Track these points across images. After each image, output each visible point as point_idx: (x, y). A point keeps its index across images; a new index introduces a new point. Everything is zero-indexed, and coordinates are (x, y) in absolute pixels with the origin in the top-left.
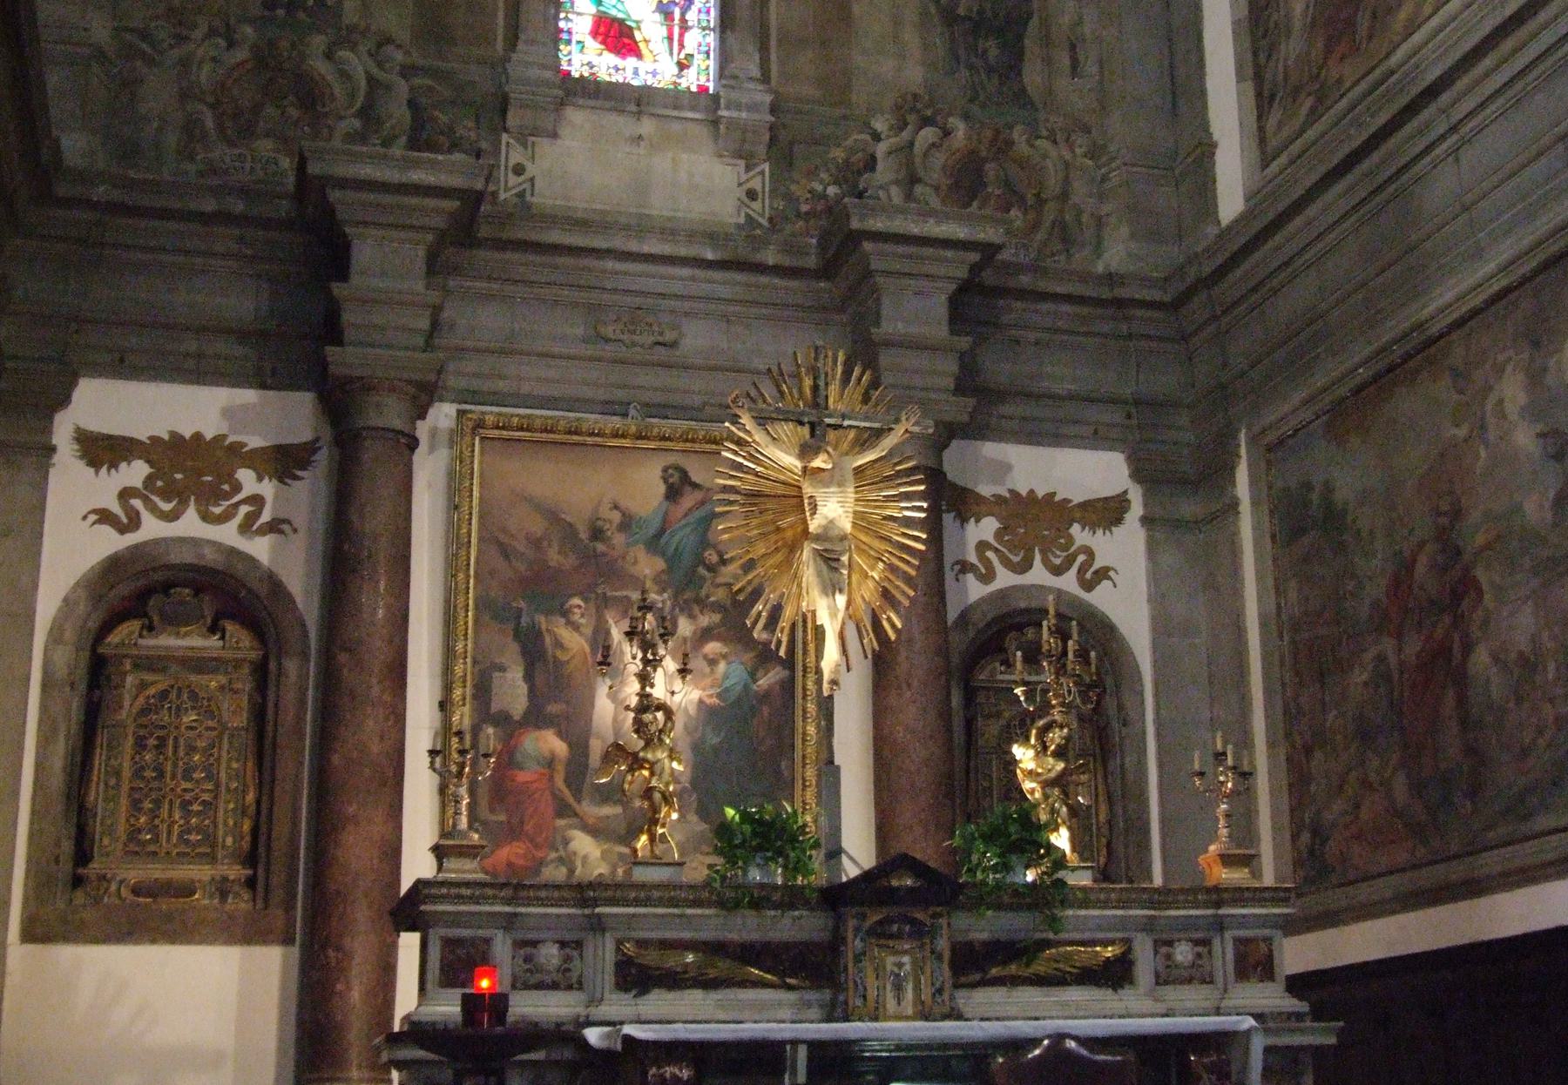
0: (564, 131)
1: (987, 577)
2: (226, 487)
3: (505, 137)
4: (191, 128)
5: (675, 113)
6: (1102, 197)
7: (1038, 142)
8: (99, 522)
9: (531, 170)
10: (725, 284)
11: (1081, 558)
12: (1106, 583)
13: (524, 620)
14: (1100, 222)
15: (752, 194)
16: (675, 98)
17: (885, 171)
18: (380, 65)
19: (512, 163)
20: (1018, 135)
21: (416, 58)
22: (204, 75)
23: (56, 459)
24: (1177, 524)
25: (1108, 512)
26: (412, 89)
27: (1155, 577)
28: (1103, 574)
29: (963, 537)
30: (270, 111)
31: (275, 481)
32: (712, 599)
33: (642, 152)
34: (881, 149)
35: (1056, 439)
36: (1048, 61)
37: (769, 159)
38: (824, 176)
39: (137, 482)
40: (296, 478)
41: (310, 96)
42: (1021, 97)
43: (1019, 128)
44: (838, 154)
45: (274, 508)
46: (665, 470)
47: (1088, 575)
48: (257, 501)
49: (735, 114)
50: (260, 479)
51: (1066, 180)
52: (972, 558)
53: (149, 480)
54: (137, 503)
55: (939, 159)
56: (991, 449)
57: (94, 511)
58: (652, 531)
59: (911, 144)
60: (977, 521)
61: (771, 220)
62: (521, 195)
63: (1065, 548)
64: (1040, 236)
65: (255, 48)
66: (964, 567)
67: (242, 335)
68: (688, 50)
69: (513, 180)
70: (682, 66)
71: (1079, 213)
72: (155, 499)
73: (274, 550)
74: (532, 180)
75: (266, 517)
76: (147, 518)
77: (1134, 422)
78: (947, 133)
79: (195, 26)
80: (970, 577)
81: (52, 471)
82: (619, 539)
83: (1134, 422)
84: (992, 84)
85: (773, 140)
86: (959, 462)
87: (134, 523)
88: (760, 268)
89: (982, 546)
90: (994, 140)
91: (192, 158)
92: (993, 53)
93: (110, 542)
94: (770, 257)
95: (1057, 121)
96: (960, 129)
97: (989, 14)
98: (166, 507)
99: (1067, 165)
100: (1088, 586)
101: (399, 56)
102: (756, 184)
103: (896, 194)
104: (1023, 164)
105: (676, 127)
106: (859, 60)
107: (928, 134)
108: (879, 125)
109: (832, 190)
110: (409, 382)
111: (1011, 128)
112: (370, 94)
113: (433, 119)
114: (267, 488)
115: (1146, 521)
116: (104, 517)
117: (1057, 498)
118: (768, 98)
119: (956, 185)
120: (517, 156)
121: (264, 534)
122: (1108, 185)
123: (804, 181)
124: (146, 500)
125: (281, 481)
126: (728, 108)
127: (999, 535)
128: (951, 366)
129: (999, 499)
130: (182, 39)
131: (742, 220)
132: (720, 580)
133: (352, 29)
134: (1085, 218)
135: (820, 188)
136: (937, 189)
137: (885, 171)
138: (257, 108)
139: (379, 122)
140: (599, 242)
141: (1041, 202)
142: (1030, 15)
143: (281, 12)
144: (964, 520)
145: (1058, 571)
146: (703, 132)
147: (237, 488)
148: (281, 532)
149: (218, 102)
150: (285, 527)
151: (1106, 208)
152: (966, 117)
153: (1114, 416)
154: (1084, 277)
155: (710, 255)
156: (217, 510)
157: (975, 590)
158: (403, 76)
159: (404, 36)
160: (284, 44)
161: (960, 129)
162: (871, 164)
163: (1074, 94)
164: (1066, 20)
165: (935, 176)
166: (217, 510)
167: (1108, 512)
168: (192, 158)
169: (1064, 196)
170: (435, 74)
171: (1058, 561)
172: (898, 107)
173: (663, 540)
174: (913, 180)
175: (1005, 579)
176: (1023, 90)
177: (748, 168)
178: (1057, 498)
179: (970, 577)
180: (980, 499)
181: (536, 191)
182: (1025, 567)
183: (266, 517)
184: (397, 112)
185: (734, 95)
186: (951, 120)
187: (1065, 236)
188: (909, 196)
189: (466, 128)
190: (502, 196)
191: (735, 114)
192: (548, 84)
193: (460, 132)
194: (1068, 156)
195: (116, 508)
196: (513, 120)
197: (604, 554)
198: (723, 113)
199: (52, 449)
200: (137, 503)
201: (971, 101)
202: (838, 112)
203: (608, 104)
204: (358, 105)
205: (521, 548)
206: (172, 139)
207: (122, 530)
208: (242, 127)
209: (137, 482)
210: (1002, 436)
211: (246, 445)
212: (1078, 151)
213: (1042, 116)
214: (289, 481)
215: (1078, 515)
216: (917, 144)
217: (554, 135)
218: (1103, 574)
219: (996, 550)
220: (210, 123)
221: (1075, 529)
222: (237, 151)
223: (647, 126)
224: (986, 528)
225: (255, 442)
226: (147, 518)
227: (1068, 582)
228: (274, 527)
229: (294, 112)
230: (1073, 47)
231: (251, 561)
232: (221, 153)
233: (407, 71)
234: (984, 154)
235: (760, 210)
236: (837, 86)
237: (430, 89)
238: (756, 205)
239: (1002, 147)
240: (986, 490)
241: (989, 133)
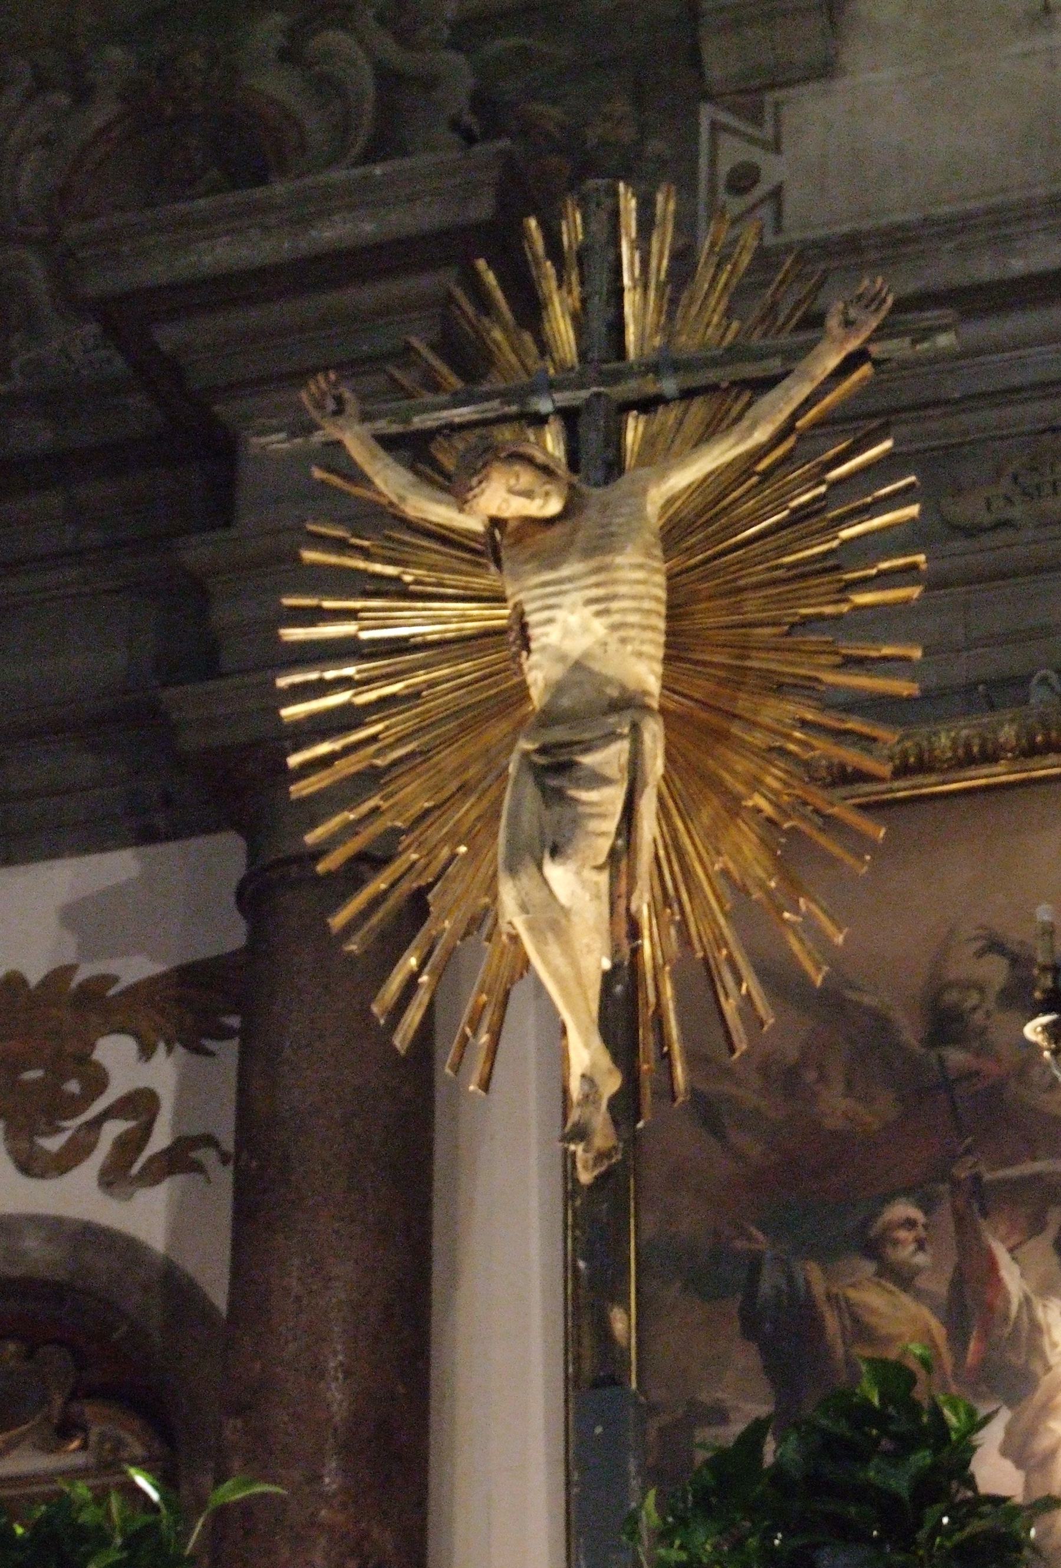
2: (73, 1087)
3: (706, 113)
13: (769, 1282)
19: (724, 169)
31: (179, 1050)
45: (179, 1114)
74: (777, 194)
75: (160, 1139)
121: (156, 1181)
147: (98, 1081)
148: (197, 1167)
156: (53, 1144)
158: (455, 45)
166: (53, 1144)
181: (786, 222)
211: (114, 980)
214: (210, 1044)
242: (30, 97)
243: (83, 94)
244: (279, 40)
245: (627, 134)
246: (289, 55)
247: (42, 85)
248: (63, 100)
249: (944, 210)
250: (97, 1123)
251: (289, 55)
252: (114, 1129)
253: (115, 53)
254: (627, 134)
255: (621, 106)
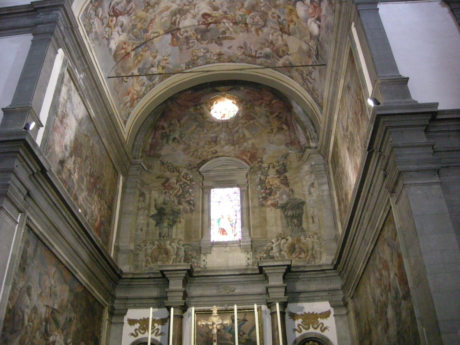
0: (212, 252)
1: (300, 331)
4: (147, 261)
5: (233, 245)
6: (321, 248)
7: (306, 238)
8: (131, 335)
9: (206, 260)
10: (241, 278)
11: (321, 325)
12: (327, 330)
14: (321, 253)
15: (249, 259)
16: (233, 242)
17: (275, 250)
18: (179, 245)
20: (302, 238)
21: (185, 243)
22: (149, 251)
23: (124, 324)
24: (341, 316)
25: (326, 315)
26: (185, 248)
27: (337, 327)
28: (326, 328)
29: (295, 324)
30: (160, 256)
32: (242, 342)
33: (227, 253)
34: (274, 245)
35: (313, 301)
36: (308, 222)
37: (251, 251)
38: (263, 253)
39: (138, 328)
40: (165, 324)
41: (167, 253)
42: (303, 230)
43: (302, 236)
44: (265, 248)
46: (231, 317)
47: (323, 329)
48: (158, 329)
49: (244, 244)
50: (158, 325)
51: (313, 246)
52: (297, 328)
53: (140, 327)
54: (138, 331)
55: (286, 245)
56: (300, 304)
57: (131, 333)
58: (230, 328)
59: (280, 244)
60: (297, 320)
61: (252, 263)
62: (205, 265)
63: (317, 323)
64: (308, 257)
65: (158, 245)
66: (295, 330)
67: (155, 298)
68: (236, 232)
69: (203, 263)
70: (235, 235)
71: (316, 251)
72: (141, 330)
73: (161, 339)
74: (207, 262)
75: (159, 332)
76: (139, 334)
77: (330, 295)
78: (287, 240)
79: (147, 243)
80: (296, 332)
81: (124, 327)
82: (223, 331)
83: (330, 295)
84: (296, 229)
85: (252, 248)
86: (291, 307)
87: (137, 335)
88: (248, 274)
89: (299, 325)
90: (297, 239)
91: (147, 267)
92: (296, 222)
93: (133, 339)
94: (249, 272)
95: (310, 233)
96: (290, 239)
97: (295, 214)
98: (142, 332)
99: (313, 242)
100: (322, 331)
101: (182, 243)
102: (249, 257)
103: (277, 254)
104: (303, 244)
105: (233, 248)
106: (268, 228)
107: (284, 241)
108: (273, 241)
109: (264, 255)
110: (180, 306)
111: (300, 236)
112: (177, 250)
113: (188, 253)
114: (160, 327)
115: (334, 315)
116: (132, 334)
117: (315, 313)
118: (250, 240)
119: (290, 251)
120: (203, 257)
122: (321, 245)
123: (259, 255)
124: (139, 331)
125: (162, 325)
126: (244, 242)
127: (302, 322)
128: (283, 290)
129: (302, 315)
130: (145, 245)
131: (247, 264)
132: (243, 338)
133: (174, 239)
134: (317, 252)
135: (262, 255)
136: (286, 252)
137: (275, 250)
138: (158, 256)
139: (179, 255)
140: (217, 274)
141: (308, 251)
142: (303, 213)
143: (162, 238)
144: (294, 320)
145: (315, 329)
146: (239, 248)
148: (162, 335)
149: (151, 256)
150: (163, 334)
151: (322, 250)
152: (291, 236)
153: (326, 294)
154: (314, 266)
155: (237, 273)
157: (298, 335)
159: (183, 238)
160: (162, 244)
161: (290, 239)
162: (272, 249)
163: (313, 227)
164: (311, 212)
165: (285, 249)
167: (326, 315)
168: (147, 267)
169: (313, 249)
170: (188, 245)
171: (315, 327)
172: (277, 236)
173: (232, 331)
174: (281, 250)
175: (304, 331)
176: (303, 228)
177: (247, 254)
178: (315, 313)
179: (296, 332)
180: (298, 315)
182: (308, 328)
183: (159, 332)
184: (182, 253)
185: (243, 240)
186: (288, 237)
187: (314, 257)
188: (280, 254)
189: (194, 254)
190: (201, 266)
191: (244, 244)
192: (208, 244)
193: (193, 255)
194: (313, 240)
195: (134, 333)
196: (202, 252)
197: (221, 335)
198: (241, 244)
199: (124, 323)
200: (138, 331)
201: (292, 232)
202: (265, 239)
203: (220, 245)
204: (175, 253)
205: (204, 334)
206: (144, 264)
207: (135, 336)
208: (155, 260)
209: (138, 328)
210: (301, 301)
212: (315, 239)
213: (307, 233)
215: (319, 316)
216: (281, 244)
217: (210, 253)
218: (326, 328)
219: (302, 326)
220: (150, 260)
221: (319, 319)
222: (154, 264)
223: (228, 249)
224: (299, 321)
225: (158, 318)
226: (139, 334)
227: (318, 331)
228: (161, 334)
229: (164, 256)
230: (313, 218)
231: (157, 341)
232: (152, 265)
233: (184, 245)
234: (295, 243)
235: (250, 262)
236: (265, 235)
237: (188, 248)
238: (250, 261)
239: (299, 240)
240: (299, 313)
241: (296, 238)
242: (150, 244)
243: (154, 245)
244: (169, 243)
245: (196, 255)
246: (170, 245)
247: (150, 243)
248: (152, 245)
249: (219, 266)
250: (155, 330)
251: (170, 245)
252: (156, 331)
253: (156, 242)
254: (196, 255)
255: (195, 253)
